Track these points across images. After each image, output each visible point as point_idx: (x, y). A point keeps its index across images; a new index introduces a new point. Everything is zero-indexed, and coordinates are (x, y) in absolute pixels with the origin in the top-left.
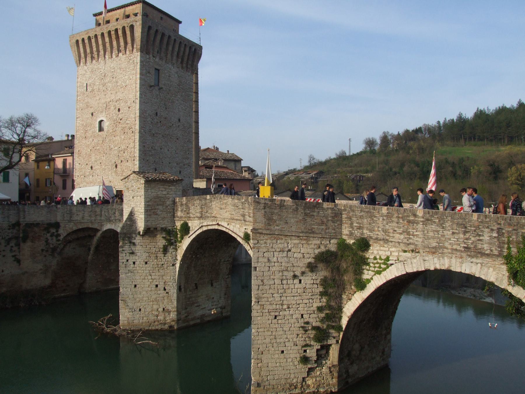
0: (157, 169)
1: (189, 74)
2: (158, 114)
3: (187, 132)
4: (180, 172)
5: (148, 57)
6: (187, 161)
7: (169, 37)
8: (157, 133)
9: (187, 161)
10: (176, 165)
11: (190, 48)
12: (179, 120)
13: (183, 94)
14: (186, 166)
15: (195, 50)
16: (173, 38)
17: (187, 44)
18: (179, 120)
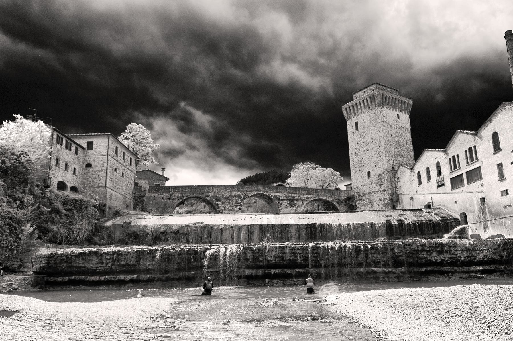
0: (361, 170)
1: (376, 109)
2: (359, 143)
3: (379, 142)
4: (376, 166)
5: (351, 120)
6: (381, 158)
7: (356, 104)
8: (359, 153)
9: (381, 158)
10: (372, 163)
11: (370, 97)
12: (372, 138)
13: (373, 123)
14: (379, 161)
15: (374, 95)
16: (358, 102)
17: (367, 97)
18: (372, 138)
